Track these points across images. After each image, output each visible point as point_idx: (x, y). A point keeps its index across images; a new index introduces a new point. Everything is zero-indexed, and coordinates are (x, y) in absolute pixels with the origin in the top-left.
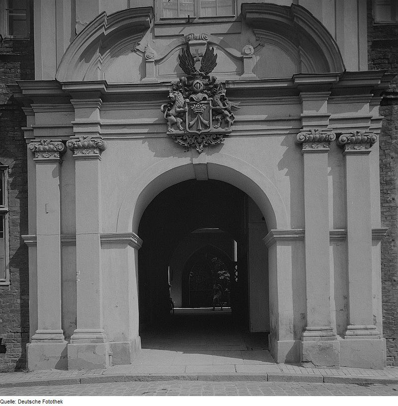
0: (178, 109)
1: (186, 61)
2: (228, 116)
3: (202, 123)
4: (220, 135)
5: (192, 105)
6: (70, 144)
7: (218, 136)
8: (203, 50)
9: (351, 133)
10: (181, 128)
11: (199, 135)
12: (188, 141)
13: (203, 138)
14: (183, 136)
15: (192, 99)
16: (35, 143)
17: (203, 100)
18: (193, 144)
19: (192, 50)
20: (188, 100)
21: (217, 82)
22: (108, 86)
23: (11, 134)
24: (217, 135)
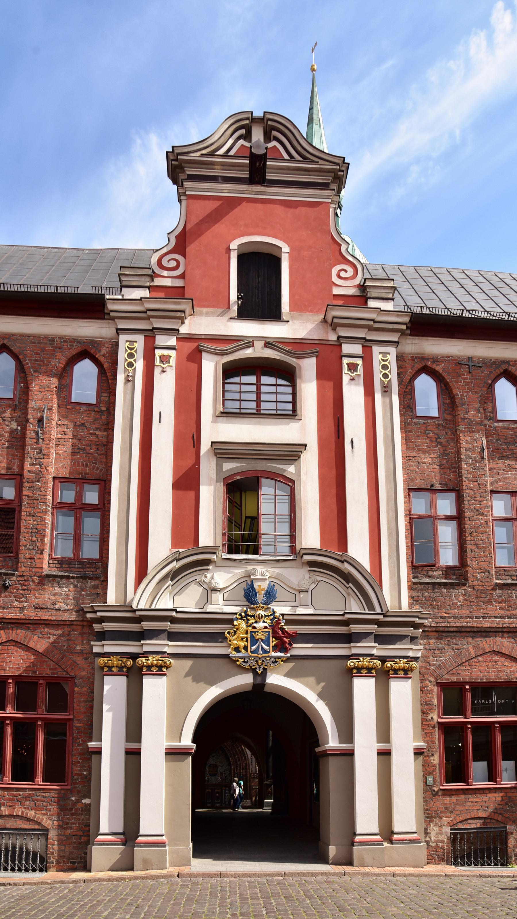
0: (241, 635)
1: (249, 594)
2: (286, 642)
3: (262, 647)
4: (279, 658)
5: (254, 632)
6: (140, 662)
7: (277, 660)
8: (265, 585)
9: (394, 661)
10: (243, 651)
11: (260, 658)
12: (249, 663)
13: (263, 661)
14: (244, 659)
15: (254, 628)
16: (105, 659)
17: (264, 629)
18: (254, 666)
19: (256, 585)
20: (250, 628)
21: (277, 615)
22: (177, 612)
23: (79, 648)
24: (275, 658)
